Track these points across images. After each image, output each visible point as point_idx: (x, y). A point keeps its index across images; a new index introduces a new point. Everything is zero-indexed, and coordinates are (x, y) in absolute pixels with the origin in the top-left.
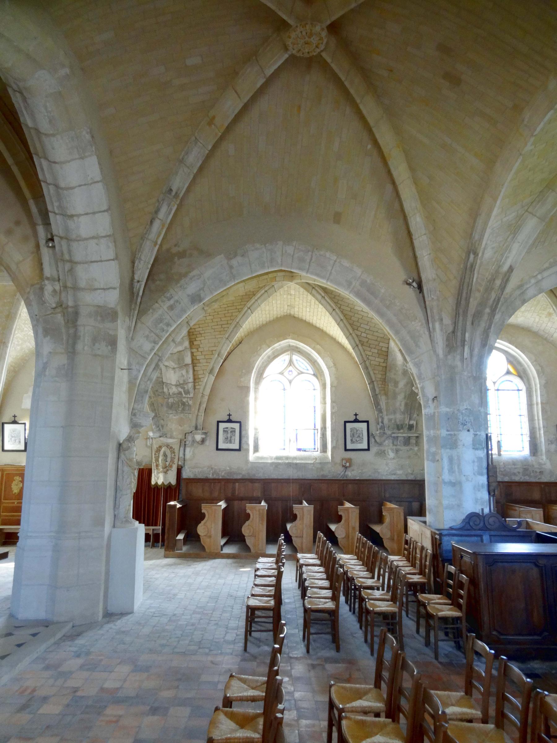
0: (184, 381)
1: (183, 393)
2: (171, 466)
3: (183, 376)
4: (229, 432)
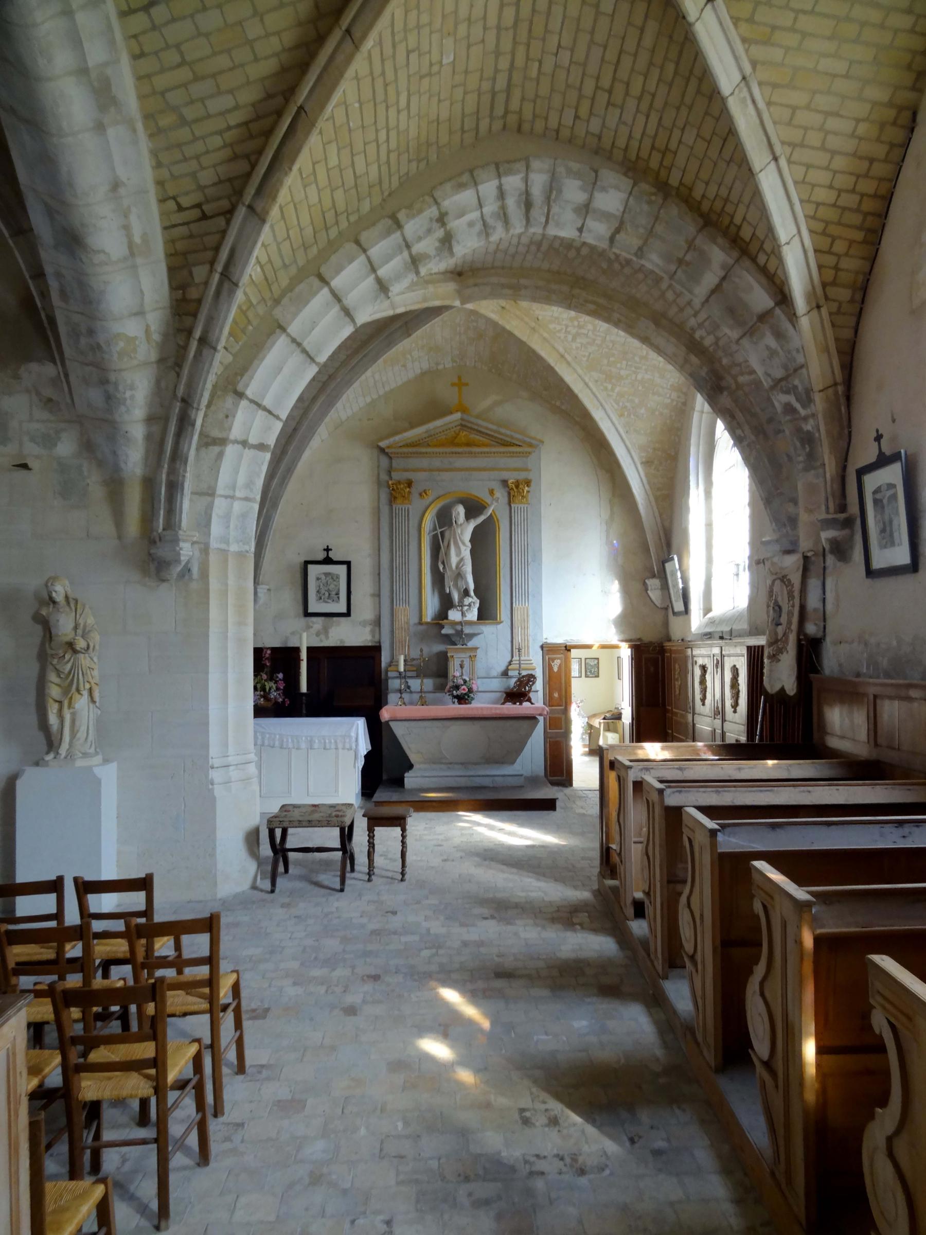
0: (785, 367)
1: (798, 406)
3: (773, 353)
4: (885, 501)
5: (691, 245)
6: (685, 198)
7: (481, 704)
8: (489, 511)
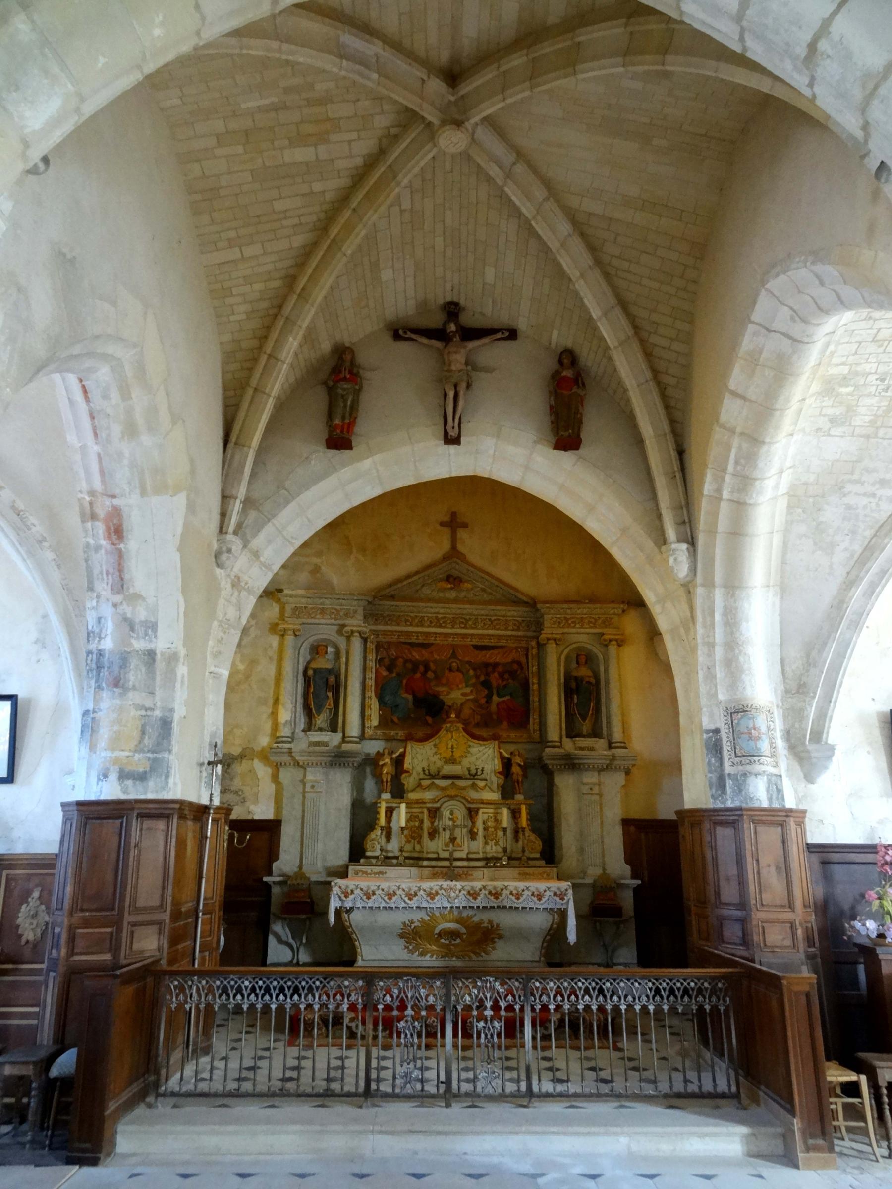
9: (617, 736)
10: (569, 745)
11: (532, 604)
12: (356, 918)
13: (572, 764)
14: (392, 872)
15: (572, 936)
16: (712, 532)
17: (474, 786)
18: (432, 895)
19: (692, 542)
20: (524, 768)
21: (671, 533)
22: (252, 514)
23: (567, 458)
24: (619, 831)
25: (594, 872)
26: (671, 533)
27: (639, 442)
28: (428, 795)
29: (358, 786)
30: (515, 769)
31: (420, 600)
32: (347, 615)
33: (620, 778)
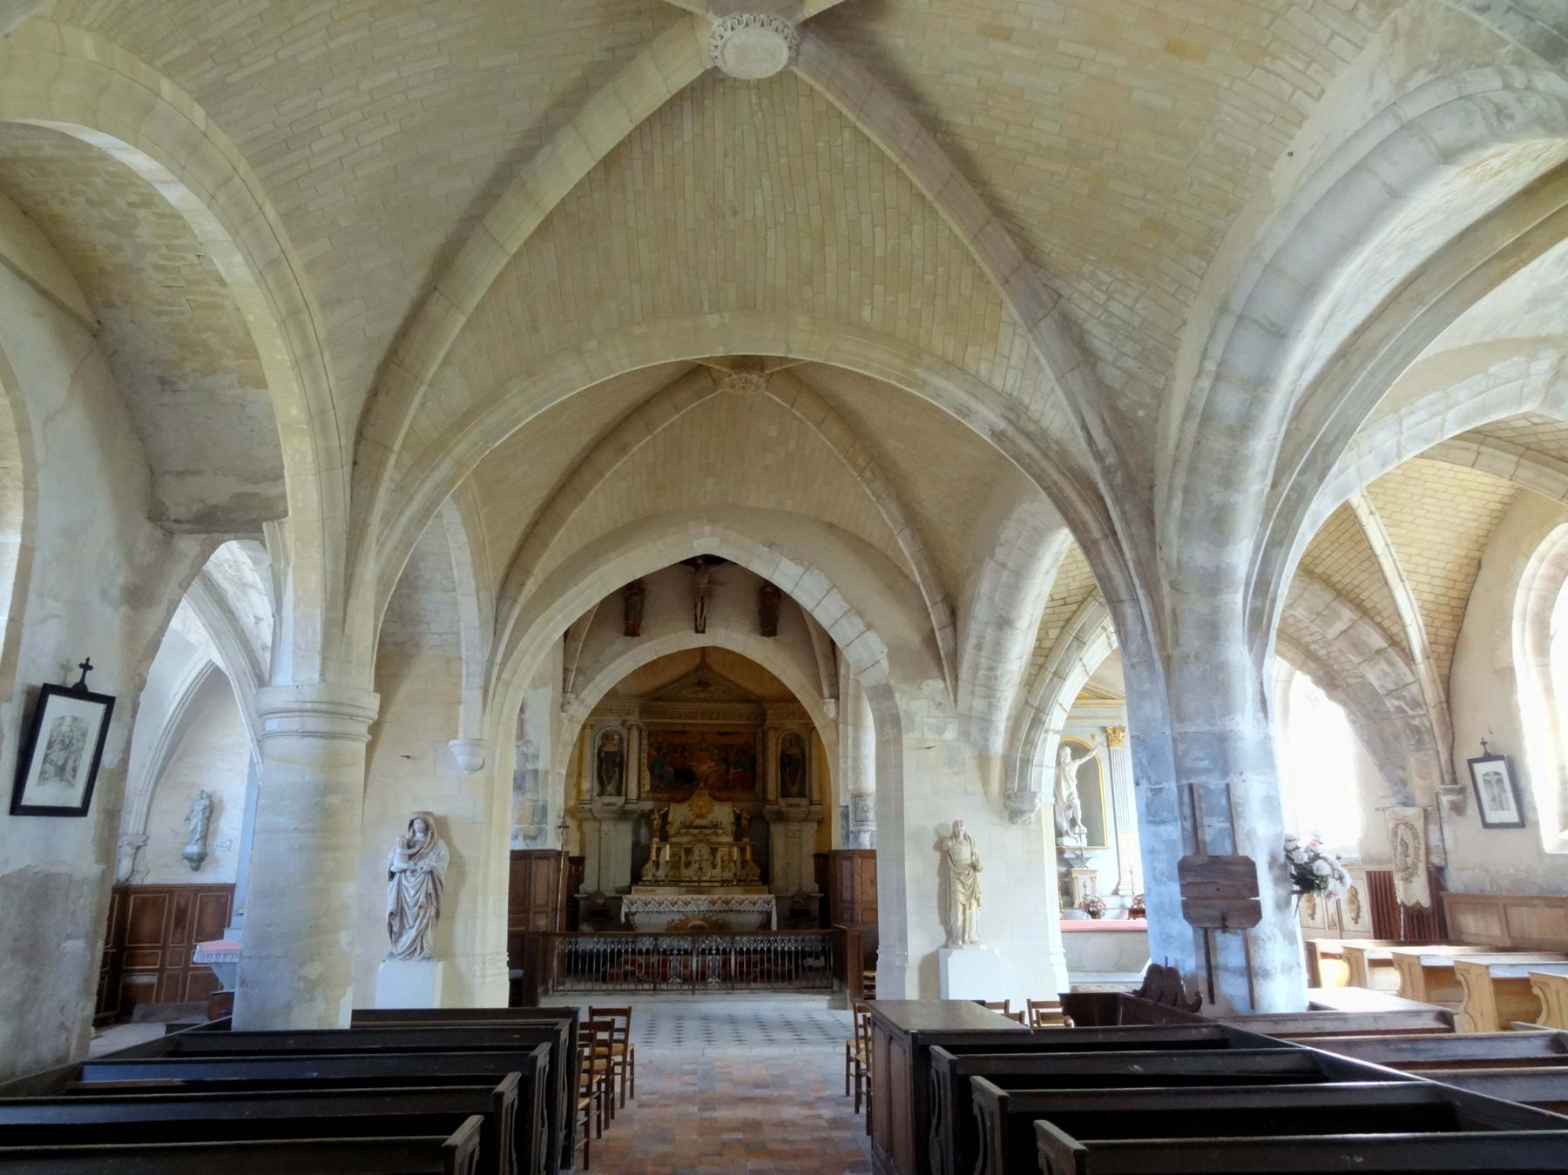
2: (1415, 866)
3: (1386, 674)
5: (1327, 606)
6: (1326, 581)
7: (1108, 919)
8: (1094, 754)
9: (816, 796)
10: (782, 802)
11: (759, 701)
12: (637, 919)
13: (781, 817)
14: (660, 890)
15: (774, 927)
16: (846, 694)
17: (716, 834)
18: (686, 904)
19: (837, 697)
20: (750, 820)
21: (826, 692)
22: (580, 678)
23: (769, 641)
24: (811, 862)
25: (793, 889)
26: (826, 692)
27: (809, 634)
28: (685, 840)
29: (636, 833)
30: (744, 821)
31: (678, 700)
32: (628, 713)
33: (815, 825)
